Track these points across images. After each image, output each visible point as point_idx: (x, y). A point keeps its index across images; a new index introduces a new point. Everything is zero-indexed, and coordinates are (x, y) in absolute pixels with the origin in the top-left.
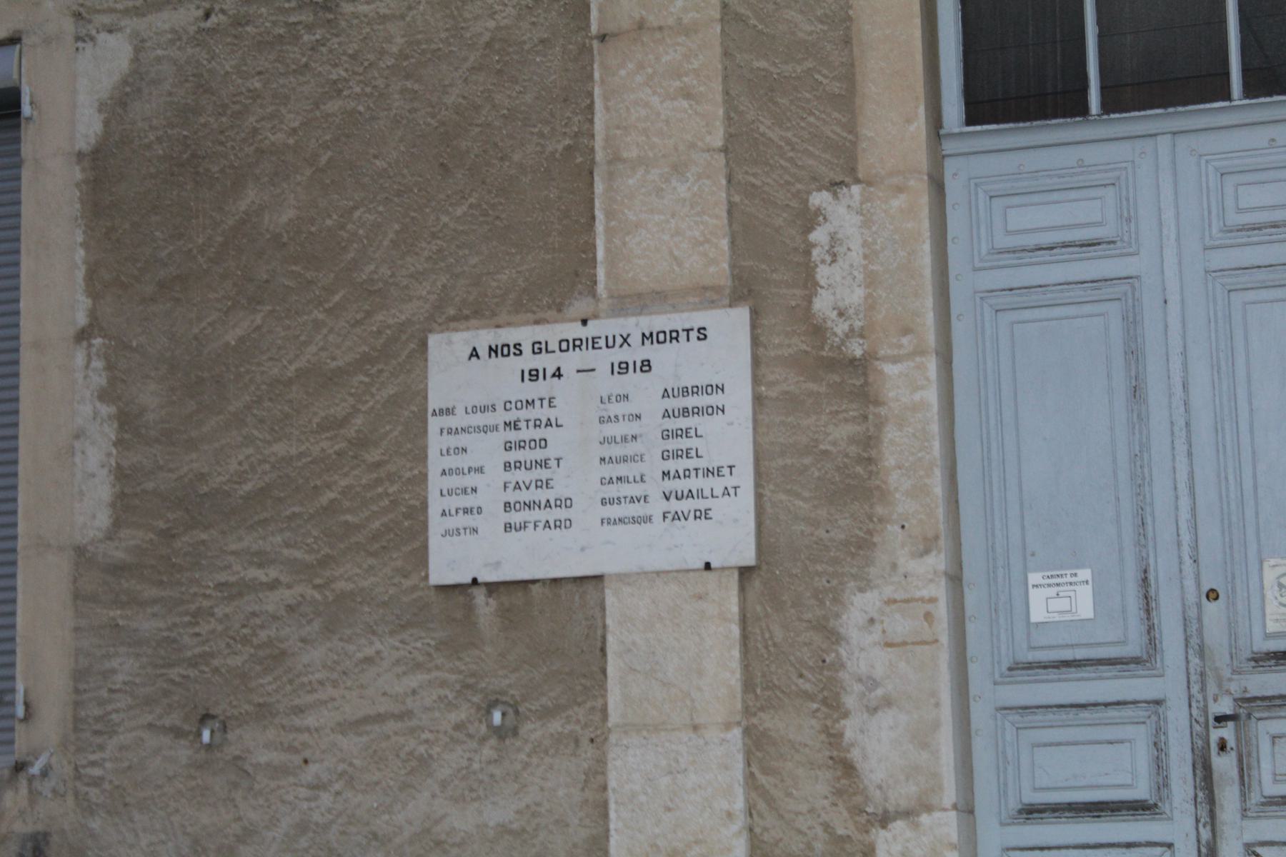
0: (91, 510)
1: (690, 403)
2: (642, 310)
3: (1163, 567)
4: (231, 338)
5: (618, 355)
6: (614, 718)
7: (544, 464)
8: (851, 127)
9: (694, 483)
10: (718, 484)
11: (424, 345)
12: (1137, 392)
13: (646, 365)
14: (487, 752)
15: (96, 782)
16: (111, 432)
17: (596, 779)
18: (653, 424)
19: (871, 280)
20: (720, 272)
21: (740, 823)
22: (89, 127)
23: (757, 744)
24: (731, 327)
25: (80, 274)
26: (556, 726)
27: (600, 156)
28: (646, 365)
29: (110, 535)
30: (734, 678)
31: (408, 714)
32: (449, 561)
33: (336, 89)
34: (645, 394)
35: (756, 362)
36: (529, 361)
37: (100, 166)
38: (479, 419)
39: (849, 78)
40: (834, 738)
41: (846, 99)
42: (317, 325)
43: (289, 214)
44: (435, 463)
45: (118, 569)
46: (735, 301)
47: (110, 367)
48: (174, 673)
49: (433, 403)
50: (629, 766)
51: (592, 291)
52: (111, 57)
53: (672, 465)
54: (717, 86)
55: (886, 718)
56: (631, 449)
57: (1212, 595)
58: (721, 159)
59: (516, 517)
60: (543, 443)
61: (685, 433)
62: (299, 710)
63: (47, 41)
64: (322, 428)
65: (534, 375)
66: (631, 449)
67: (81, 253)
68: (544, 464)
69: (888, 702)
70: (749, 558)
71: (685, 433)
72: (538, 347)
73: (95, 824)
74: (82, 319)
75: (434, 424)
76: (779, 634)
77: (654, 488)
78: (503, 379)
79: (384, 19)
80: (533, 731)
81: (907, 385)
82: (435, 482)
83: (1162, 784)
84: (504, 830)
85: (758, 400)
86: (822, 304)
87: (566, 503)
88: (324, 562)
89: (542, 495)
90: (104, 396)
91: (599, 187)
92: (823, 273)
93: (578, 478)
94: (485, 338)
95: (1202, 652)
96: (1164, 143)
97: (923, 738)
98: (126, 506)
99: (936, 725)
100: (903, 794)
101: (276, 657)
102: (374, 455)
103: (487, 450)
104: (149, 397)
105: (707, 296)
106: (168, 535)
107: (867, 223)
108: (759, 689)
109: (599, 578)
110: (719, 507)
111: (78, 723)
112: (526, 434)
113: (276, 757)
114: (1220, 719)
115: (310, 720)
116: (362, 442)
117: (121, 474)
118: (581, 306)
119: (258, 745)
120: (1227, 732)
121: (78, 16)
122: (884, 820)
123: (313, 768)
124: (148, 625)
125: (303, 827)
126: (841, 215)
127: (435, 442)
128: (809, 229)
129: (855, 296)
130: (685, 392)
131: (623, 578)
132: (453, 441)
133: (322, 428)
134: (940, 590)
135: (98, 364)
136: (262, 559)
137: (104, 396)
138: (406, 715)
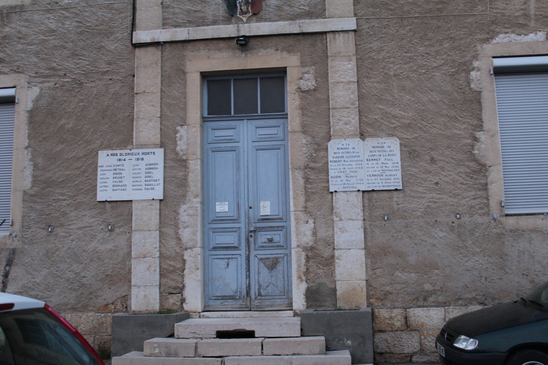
0: (27, 183)
1: (151, 167)
2: (142, 148)
3: (242, 201)
4: (58, 149)
5: (137, 157)
6: (133, 228)
7: (121, 178)
8: (185, 114)
9: (151, 183)
10: (156, 183)
11: (97, 153)
12: (238, 168)
13: (142, 159)
14: (107, 234)
15: (27, 238)
16: (32, 167)
17: (129, 240)
18: (143, 171)
19: (188, 144)
20: (158, 141)
21: (158, 249)
22: (30, 106)
23: (161, 234)
24: (160, 152)
25: (27, 135)
26: (122, 230)
27: (135, 117)
28: (142, 159)
29: (31, 188)
30: (158, 221)
31: (91, 226)
32: (101, 197)
33: (82, 101)
34: (142, 165)
35: (165, 159)
36: (119, 157)
37: (32, 114)
38: (108, 168)
39: (185, 104)
40: (177, 233)
41: (184, 109)
42: (76, 148)
43: (71, 125)
44: (99, 177)
45: (32, 195)
46: (161, 147)
47: (32, 154)
48: (43, 217)
49: (99, 165)
50: (136, 237)
51: (132, 144)
52: (35, 91)
53: (147, 179)
54: (159, 104)
55: (187, 229)
56: (139, 175)
57: (251, 208)
58: (159, 119)
59: (115, 188)
60: (121, 174)
61: (150, 173)
62: (69, 225)
63: (22, 87)
64: (76, 169)
65: (120, 160)
66: (139, 175)
67: (27, 131)
68: (121, 178)
69: (188, 226)
70: (162, 198)
71: (150, 173)
72: (121, 155)
73: (26, 247)
74: (27, 145)
75: (99, 169)
76: (167, 213)
77: (143, 183)
78: (113, 160)
79: (92, 87)
80: (117, 230)
81: (195, 166)
82: (99, 181)
83: (240, 243)
84: (110, 250)
85: (165, 167)
86: (178, 148)
87: (125, 185)
88: (76, 195)
89: (120, 184)
90: (31, 160)
91: (135, 123)
92: (178, 142)
93: (128, 181)
94: (110, 152)
95: (249, 218)
96: (245, 121)
97: (194, 233)
99: (197, 231)
100: (190, 244)
101: (64, 214)
102: (86, 175)
103: (110, 174)
104: (40, 161)
105: (155, 146)
106: (43, 189)
107: (187, 133)
108: (162, 224)
109: (131, 201)
110: (156, 188)
111: (23, 226)
112: (118, 171)
113: (64, 234)
114: (251, 231)
115: (71, 227)
116: (84, 172)
117: (34, 176)
118: (130, 147)
119: (60, 232)
120: (252, 234)
121: (28, 83)
122: (186, 249)
123: (72, 237)
124: (38, 207)
125: (69, 248)
126: (182, 131)
127: (99, 172)
128: (176, 134)
129: (184, 147)
130: (150, 164)
131: (136, 201)
132: (103, 172)
133: (76, 169)
134: (199, 205)
135: (29, 154)
136: (63, 195)
137: (31, 160)
138: (91, 226)
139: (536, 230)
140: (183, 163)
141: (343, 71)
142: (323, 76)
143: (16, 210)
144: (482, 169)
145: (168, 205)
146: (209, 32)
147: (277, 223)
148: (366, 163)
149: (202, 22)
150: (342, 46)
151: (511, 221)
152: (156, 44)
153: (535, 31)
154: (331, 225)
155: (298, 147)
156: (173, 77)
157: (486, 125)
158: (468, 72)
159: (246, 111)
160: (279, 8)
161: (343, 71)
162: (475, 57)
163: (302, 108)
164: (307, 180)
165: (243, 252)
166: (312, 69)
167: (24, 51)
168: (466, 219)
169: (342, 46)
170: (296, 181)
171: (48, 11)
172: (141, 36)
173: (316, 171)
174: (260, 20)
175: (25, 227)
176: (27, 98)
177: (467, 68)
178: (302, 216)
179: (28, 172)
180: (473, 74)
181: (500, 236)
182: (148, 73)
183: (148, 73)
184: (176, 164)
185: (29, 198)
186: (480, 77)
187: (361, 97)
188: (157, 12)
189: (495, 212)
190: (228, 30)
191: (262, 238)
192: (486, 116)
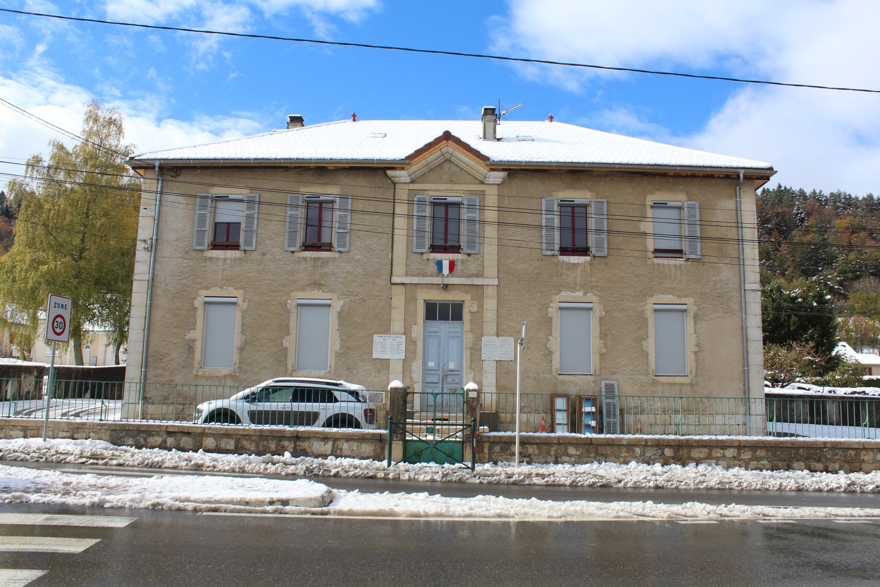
0: (337, 348)
1: (399, 344)
22: (339, 309)
32: (375, 356)
34: (395, 343)
37: (340, 313)
41: (416, 317)
52: (341, 302)
98: (341, 347)
103: (379, 346)
104: (344, 337)
119: (354, 372)
126: (414, 328)
139: (571, 382)
140: (415, 343)
141: (490, 304)
142: (481, 306)
143: (331, 360)
144: (550, 353)
145: (407, 362)
146: (428, 280)
147: (457, 373)
148: (498, 348)
149: (425, 275)
150: (491, 292)
153: (579, 291)
154: (481, 375)
155: (468, 338)
156: (410, 301)
157: (554, 333)
159: (444, 317)
160: (462, 271)
161: (490, 304)
162: (551, 302)
163: (471, 321)
164: (472, 354)
165: (440, 385)
166: (476, 302)
168: (541, 375)
169: (491, 292)
170: (466, 354)
171: (348, 262)
172: (395, 280)
173: (476, 350)
176: (338, 305)
177: (547, 306)
178: (469, 370)
179: (338, 343)
181: (556, 383)
182: (398, 298)
183: (398, 298)
184: (411, 343)
185: (338, 355)
186: (552, 311)
189: (554, 373)
190: (438, 280)
191: (449, 379)
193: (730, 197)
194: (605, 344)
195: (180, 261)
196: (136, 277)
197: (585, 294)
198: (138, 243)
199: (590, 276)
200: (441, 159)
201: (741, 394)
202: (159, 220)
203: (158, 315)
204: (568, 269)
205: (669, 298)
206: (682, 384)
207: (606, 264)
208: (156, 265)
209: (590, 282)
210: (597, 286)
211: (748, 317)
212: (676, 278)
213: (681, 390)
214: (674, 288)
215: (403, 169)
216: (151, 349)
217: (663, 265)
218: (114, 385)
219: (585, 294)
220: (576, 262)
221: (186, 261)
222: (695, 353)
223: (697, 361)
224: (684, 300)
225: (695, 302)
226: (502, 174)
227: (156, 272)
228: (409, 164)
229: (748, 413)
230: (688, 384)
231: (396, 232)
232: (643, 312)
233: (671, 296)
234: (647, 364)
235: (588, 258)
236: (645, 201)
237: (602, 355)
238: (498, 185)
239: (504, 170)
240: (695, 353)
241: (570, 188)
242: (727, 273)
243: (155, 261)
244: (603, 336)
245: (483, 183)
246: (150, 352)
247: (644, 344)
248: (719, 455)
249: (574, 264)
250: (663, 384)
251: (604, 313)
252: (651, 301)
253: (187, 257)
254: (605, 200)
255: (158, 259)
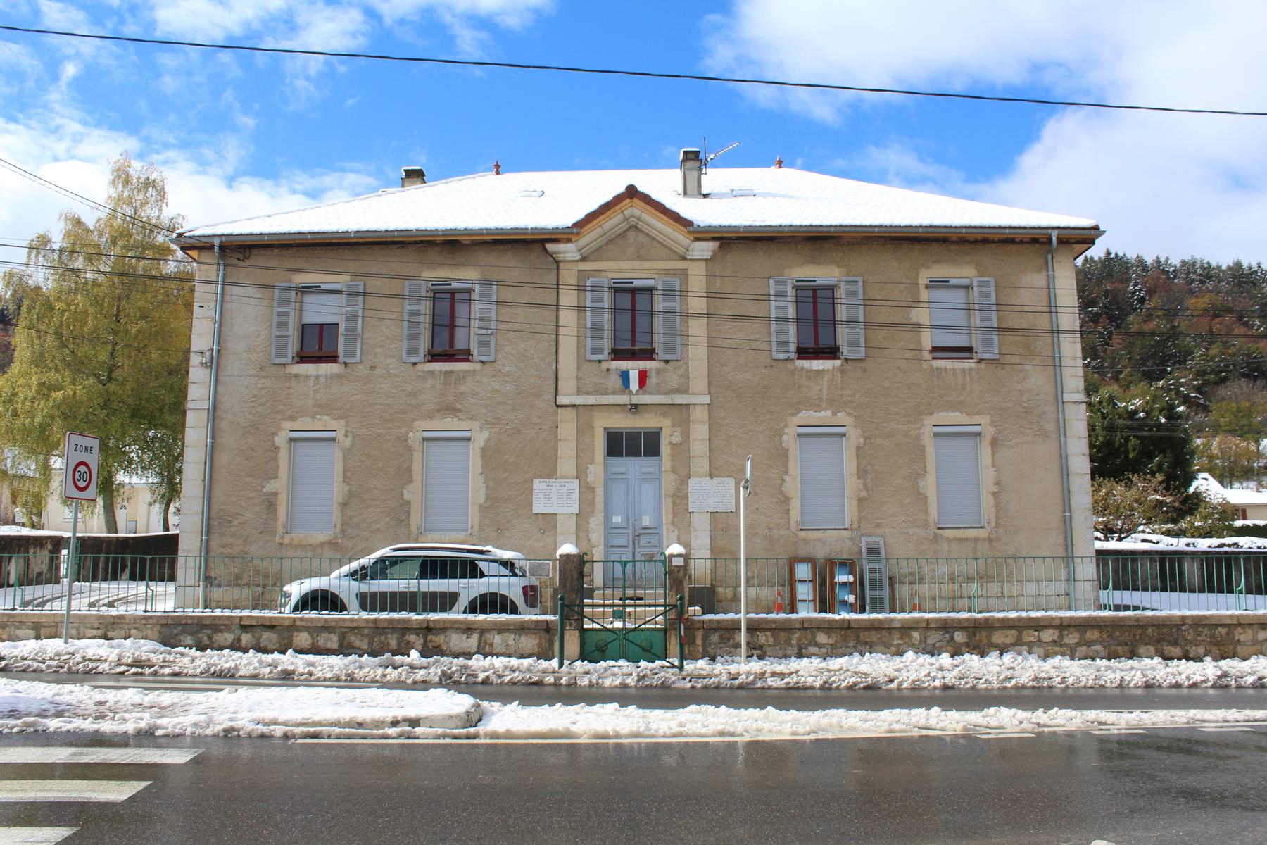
0: (482, 499)
1: (570, 491)
22: (482, 445)
32: (536, 510)
34: (564, 490)
41: (593, 452)
52: (486, 434)
98: (488, 497)
103: (542, 495)
104: (491, 484)
126: (591, 468)
139: (818, 540)
140: (592, 489)
141: (700, 431)
142: (686, 435)
143: (473, 517)
144: (787, 500)
145: (581, 518)
148: (711, 494)
149: (604, 392)
150: (699, 415)
151: (803, 533)
152: (574, 406)
153: (825, 409)
155: (669, 482)
156: (584, 430)
158: (781, 436)
159: (634, 452)
160: (658, 385)
161: (700, 431)
162: (786, 426)
164: (674, 504)
165: (630, 549)
167: (476, 404)
168: (775, 532)
169: (699, 415)
170: (667, 504)
171: (494, 376)
172: (562, 400)
173: (680, 498)
174: (644, 393)
175: (481, 529)
176: (480, 438)
177: (780, 433)
178: (671, 527)
179: (483, 492)
180: (784, 437)
182: (568, 427)
183: (568, 427)
184: (586, 490)
185: (482, 509)
186: (788, 440)
187: (711, 450)
188: (574, 382)
190: (623, 399)
191: (643, 541)
192: (791, 465)
193: (1039, 270)
194: (865, 484)
195: (253, 380)
196: (190, 405)
197: (834, 414)
198: (192, 355)
199: (842, 388)
200: (624, 226)
201: (1061, 552)
202: (221, 322)
203: (223, 459)
204: (809, 378)
205: (956, 417)
206: (976, 539)
207: (864, 370)
208: (220, 388)
209: (842, 396)
210: (852, 402)
211: (1069, 440)
212: (964, 387)
213: (975, 548)
214: (961, 403)
215: (569, 241)
216: (215, 507)
217: (946, 369)
218: (163, 560)
219: (834, 414)
220: (821, 368)
221: (262, 381)
222: (994, 494)
223: (997, 505)
224: (976, 419)
225: (992, 421)
226: (712, 245)
227: (219, 397)
228: (578, 234)
229: (1071, 578)
230: (984, 539)
231: (561, 331)
232: (918, 437)
233: (957, 414)
234: (926, 512)
235: (837, 363)
236: (917, 278)
237: (860, 500)
238: (706, 260)
239: (714, 239)
240: (994, 494)
241: (810, 262)
242: (1037, 379)
243: (217, 381)
244: (861, 473)
245: (684, 259)
246: (213, 512)
247: (921, 483)
248: (1032, 639)
249: (818, 371)
250: (949, 540)
251: (862, 441)
252: (929, 421)
253: (263, 374)
254: (860, 279)
255: (221, 379)
